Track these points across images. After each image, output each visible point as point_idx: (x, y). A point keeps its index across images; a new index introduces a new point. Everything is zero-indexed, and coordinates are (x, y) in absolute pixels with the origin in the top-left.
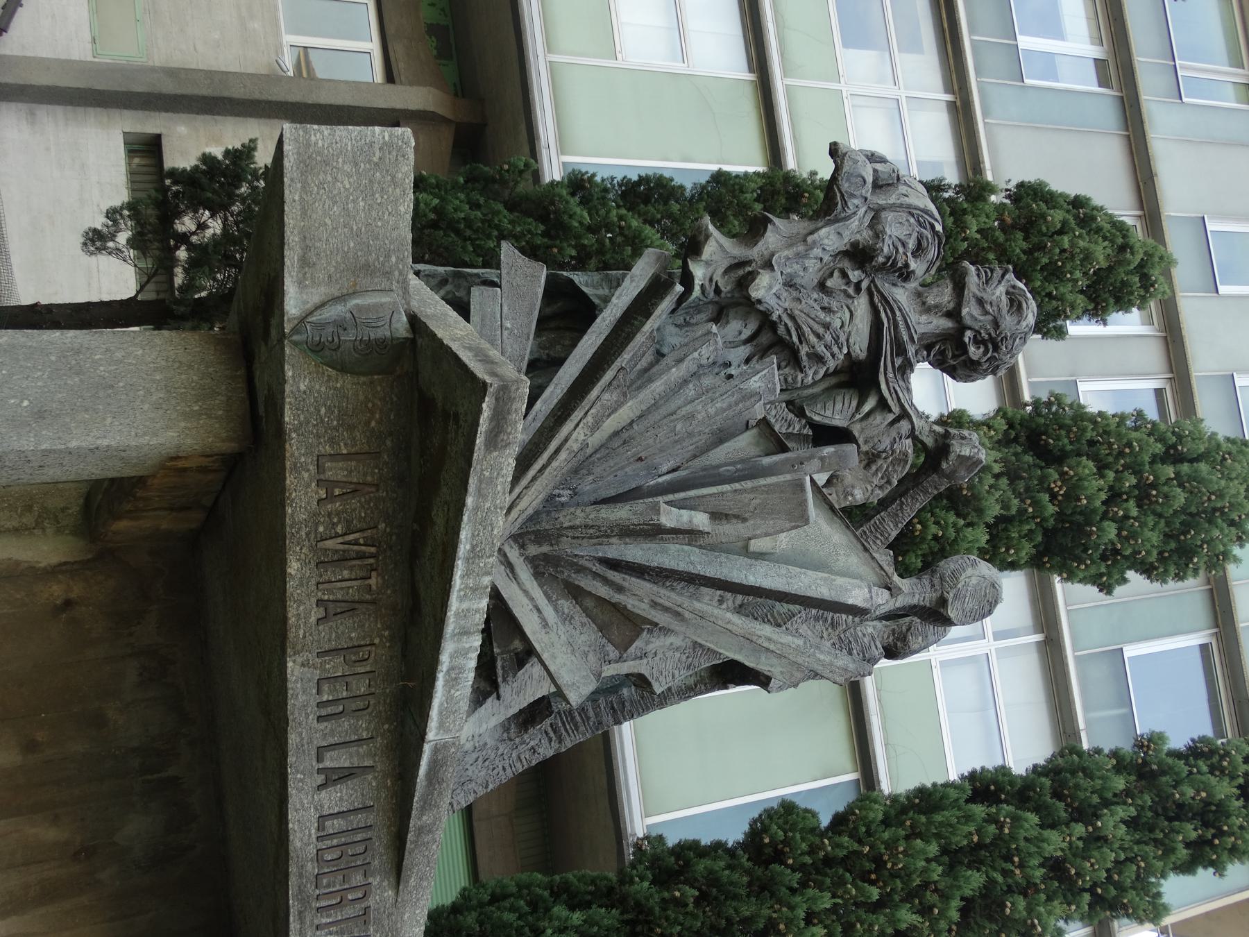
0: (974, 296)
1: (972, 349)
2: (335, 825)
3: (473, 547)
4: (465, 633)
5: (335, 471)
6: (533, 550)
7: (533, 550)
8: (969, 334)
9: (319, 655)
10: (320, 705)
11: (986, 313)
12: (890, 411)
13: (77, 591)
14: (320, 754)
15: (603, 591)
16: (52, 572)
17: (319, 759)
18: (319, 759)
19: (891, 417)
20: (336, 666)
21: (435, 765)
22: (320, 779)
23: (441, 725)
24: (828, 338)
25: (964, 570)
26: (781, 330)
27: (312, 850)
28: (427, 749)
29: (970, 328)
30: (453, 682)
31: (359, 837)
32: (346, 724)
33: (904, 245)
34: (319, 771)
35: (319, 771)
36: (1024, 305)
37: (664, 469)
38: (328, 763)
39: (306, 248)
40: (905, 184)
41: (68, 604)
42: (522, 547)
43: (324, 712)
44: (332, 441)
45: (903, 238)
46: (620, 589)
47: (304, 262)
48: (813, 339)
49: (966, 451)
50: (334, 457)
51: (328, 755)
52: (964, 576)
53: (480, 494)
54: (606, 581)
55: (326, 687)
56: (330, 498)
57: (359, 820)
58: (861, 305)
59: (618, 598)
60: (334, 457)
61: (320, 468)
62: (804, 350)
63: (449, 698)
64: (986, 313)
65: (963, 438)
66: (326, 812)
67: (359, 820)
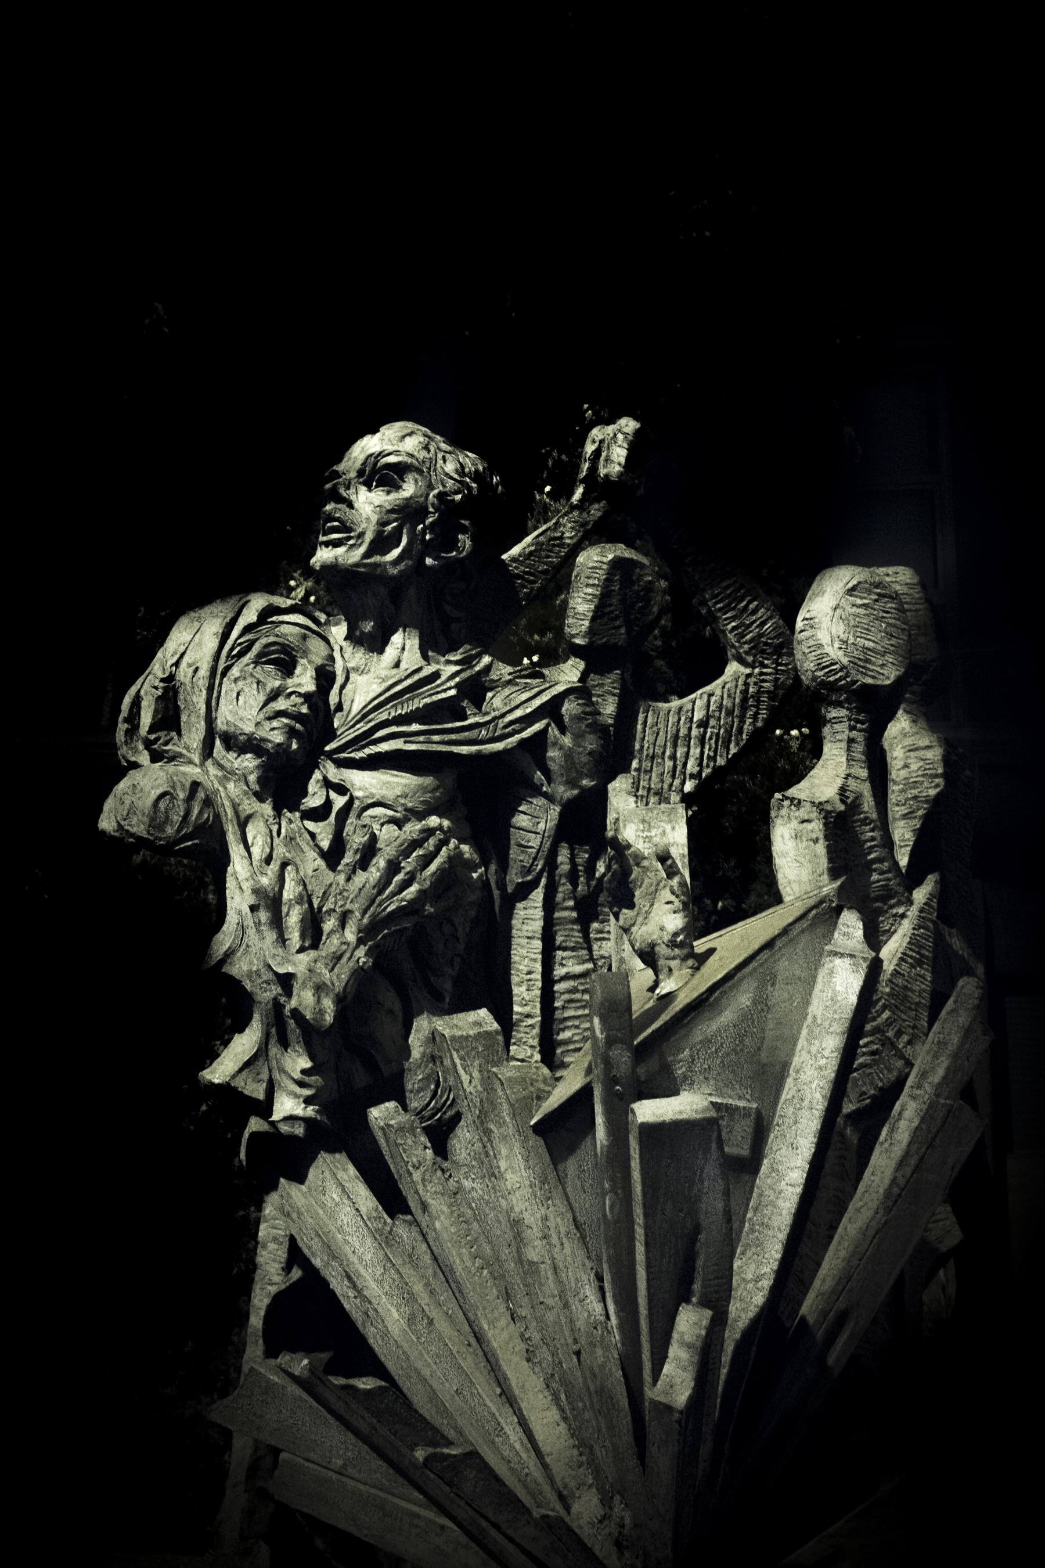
0: (367, 555)
12: (544, 732)
19: (554, 731)
25: (820, 646)
33: (274, 695)
36: (392, 459)
37: (598, 1308)
40: (177, 664)
45: (262, 698)
49: (619, 454)
52: (828, 649)
58: (365, 783)
65: (597, 453)
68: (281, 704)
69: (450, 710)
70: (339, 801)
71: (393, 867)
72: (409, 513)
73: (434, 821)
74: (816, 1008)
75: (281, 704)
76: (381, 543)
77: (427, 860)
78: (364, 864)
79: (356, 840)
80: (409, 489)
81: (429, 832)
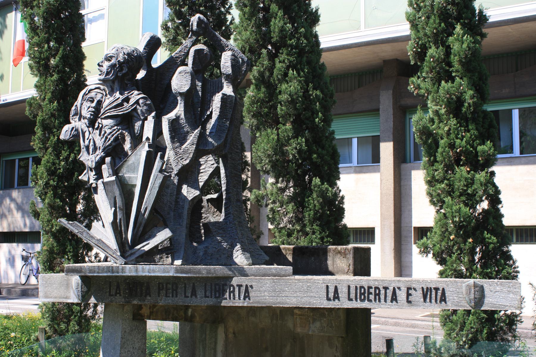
0: (106, 76)
1: (124, 72)
2: (208, 294)
3: (109, 272)
4: (137, 270)
5: (113, 292)
6: (127, 248)
7: (127, 248)
8: (119, 74)
9: (159, 296)
10: (173, 296)
11: (111, 71)
12: (136, 107)
13: (231, 330)
14: (186, 297)
15: (141, 229)
16: (226, 336)
17: (188, 297)
18: (188, 297)
19: (138, 107)
20: (163, 292)
21: (182, 273)
22: (194, 297)
23: (168, 272)
24: (109, 137)
26: (109, 151)
27: (214, 300)
28: (175, 275)
29: (117, 73)
30: (154, 271)
31: (213, 287)
32: (179, 290)
33: (88, 108)
34: (191, 297)
35: (191, 297)
36: (109, 55)
38: (190, 295)
39: (63, 298)
41: (234, 333)
42: (127, 251)
43: (175, 295)
44: (106, 293)
46: (141, 224)
47: (67, 298)
48: (110, 142)
50: (110, 292)
51: (187, 295)
53: (94, 272)
54: (139, 227)
55: (168, 295)
56: (119, 293)
57: (208, 288)
58: (106, 122)
59: (143, 225)
60: (110, 292)
61: (112, 295)
62: (113, 144)
63: (159, 271)
64: (111, 71)
66: (204, 296)
67: (208, 288)
68: (90, 109)
69: (121, 105)
70: (100, 126)
71: (106, 138)
72: (113, 66)
73: (116, 127)
74: (141, 160)
75: (90, 109)
76: (108, 73)
77: (113, 135)
78: (103, 137)
79: (103, 133)
80: (113, 61)
81: (115, 130)
